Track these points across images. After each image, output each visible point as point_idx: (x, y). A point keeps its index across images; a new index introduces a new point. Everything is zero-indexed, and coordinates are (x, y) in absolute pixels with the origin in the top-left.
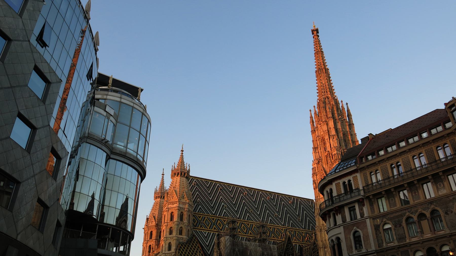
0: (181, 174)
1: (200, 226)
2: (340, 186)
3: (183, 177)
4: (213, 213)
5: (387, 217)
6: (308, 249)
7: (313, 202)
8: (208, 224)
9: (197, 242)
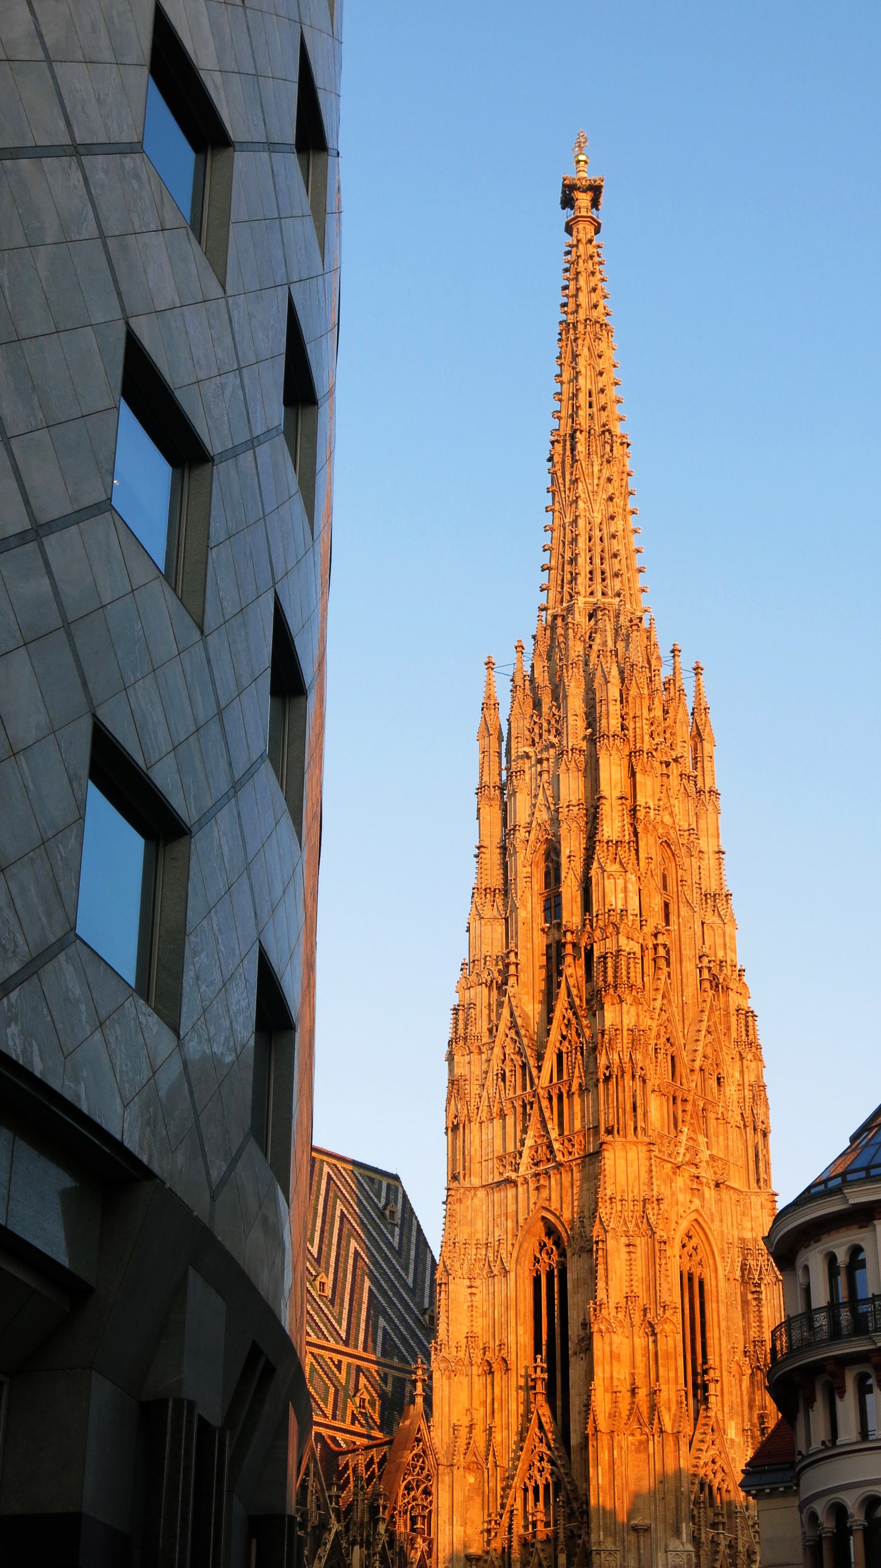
6: (375, 1466)
7: (397, 1188)
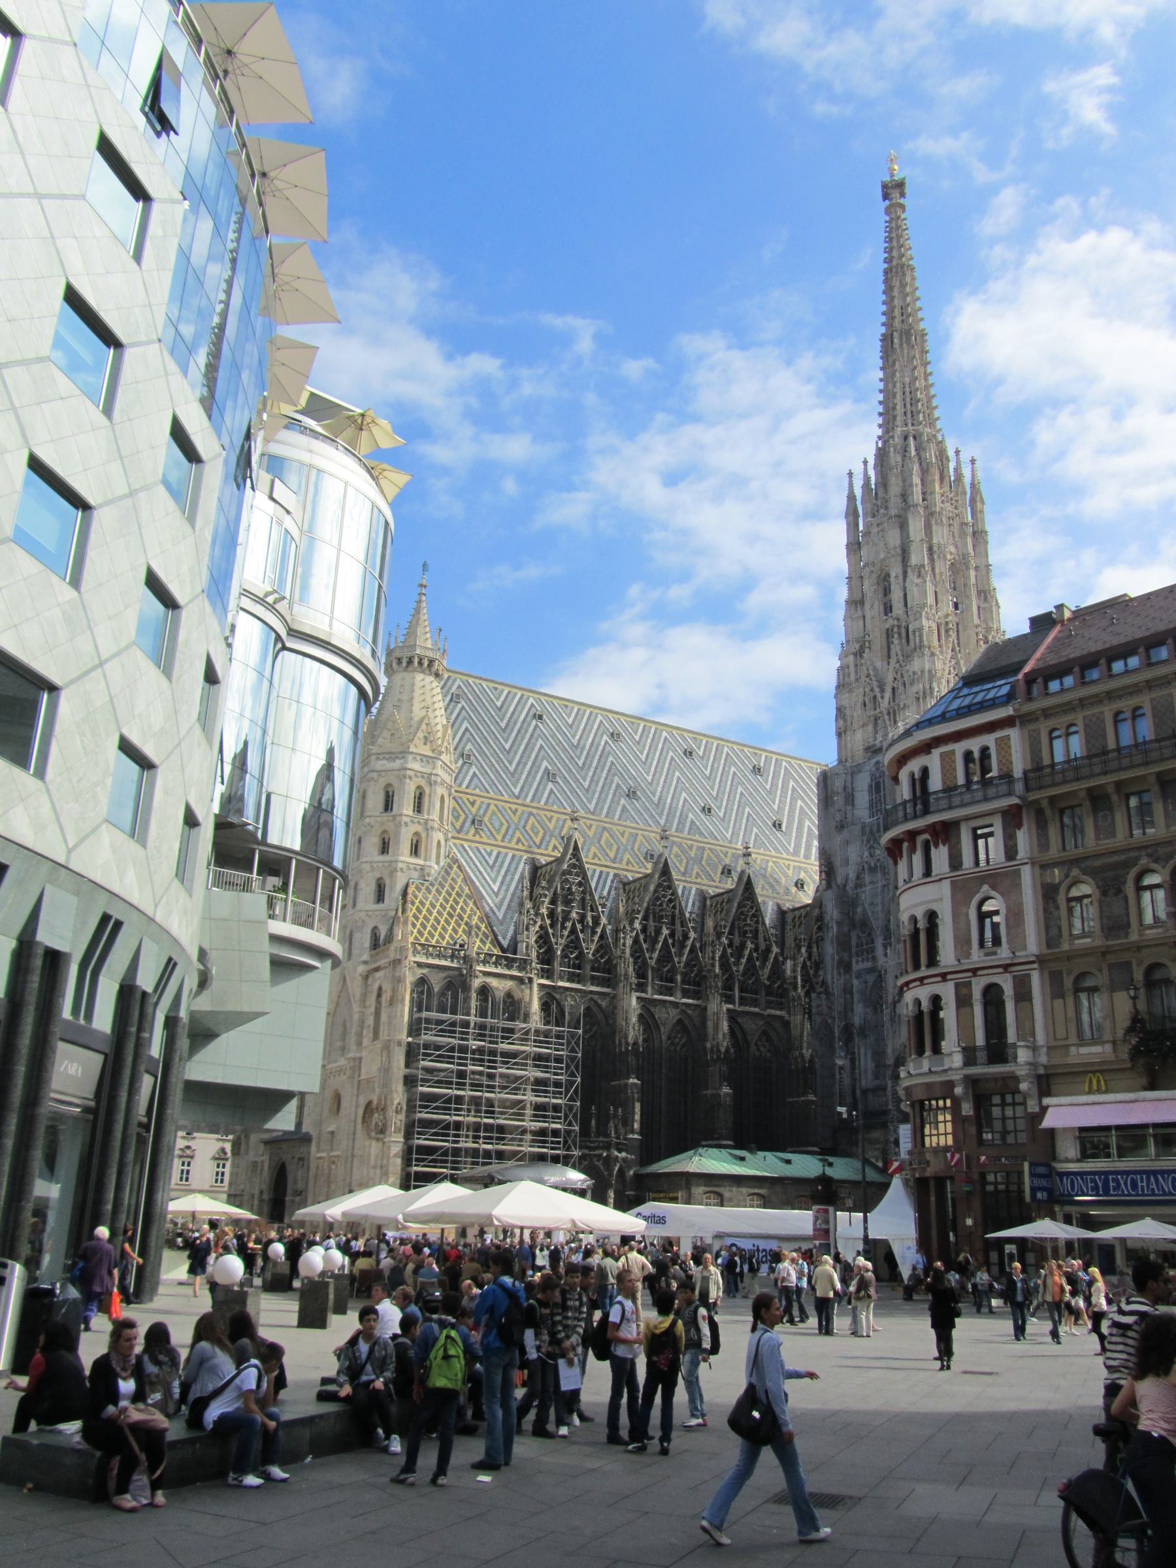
0: (420, 663)
1: (473, 831)
2: (954, 761)
3: (423, 672)
5: (1083, 865)
8: (497, 825)
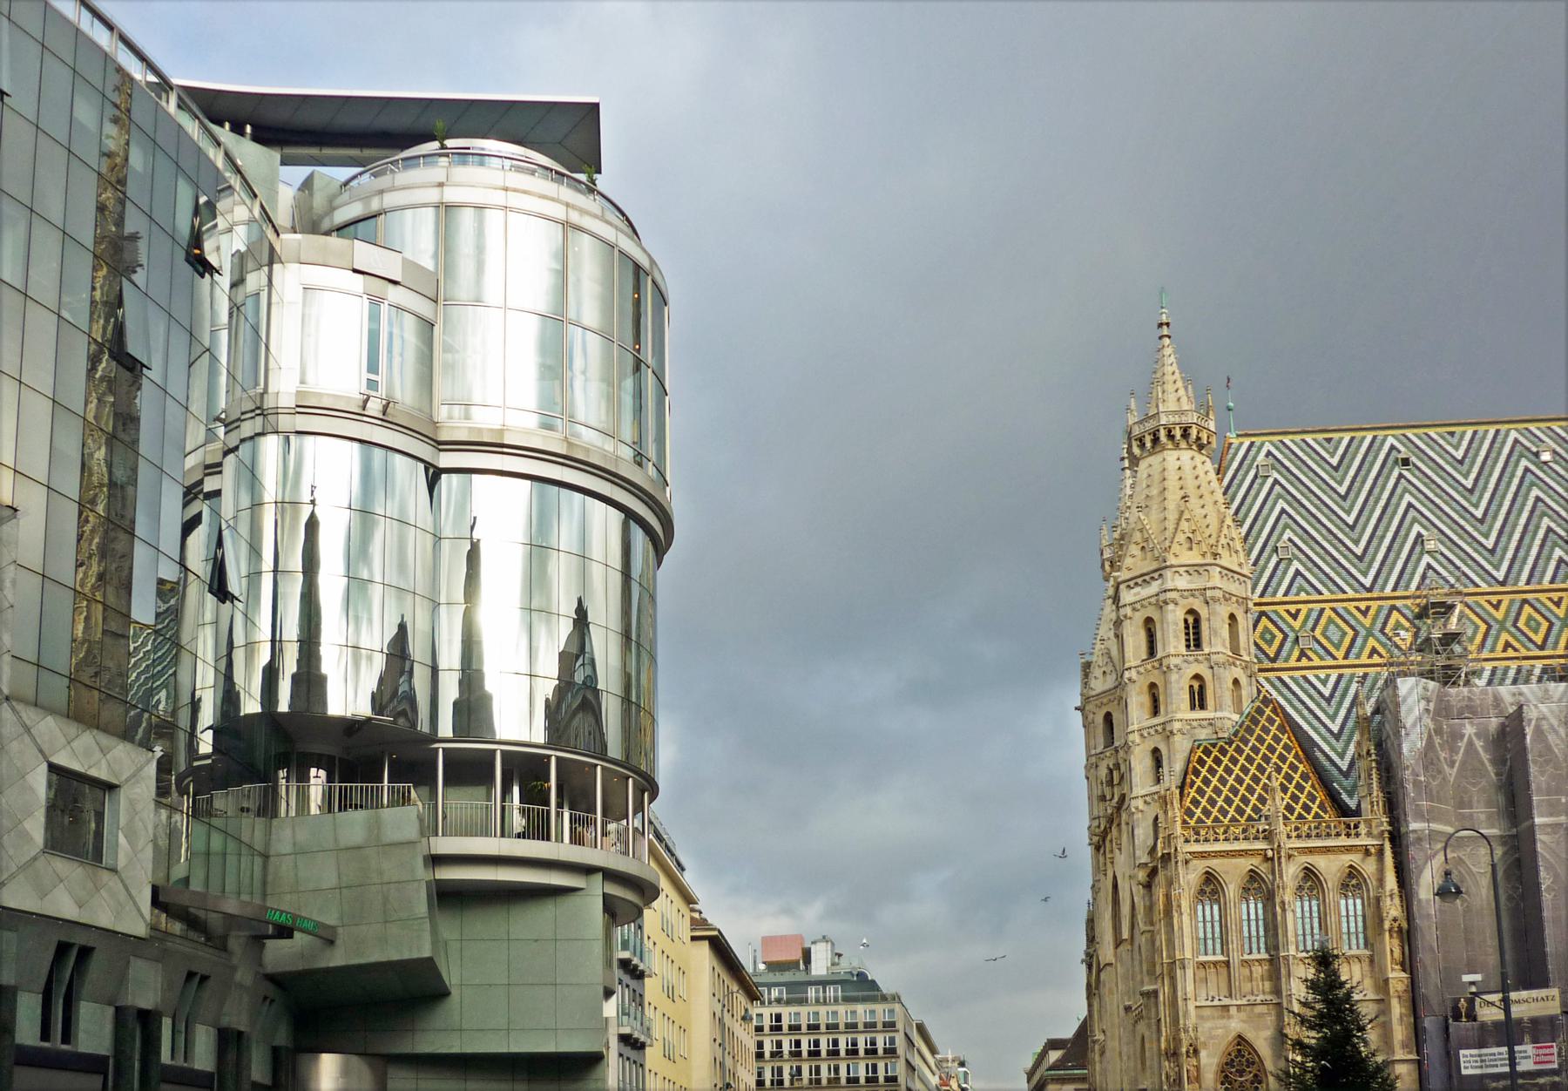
1: (1296, 653)
4: (1362, 585)
8: (1335, 639)
9: (1284, 727)
